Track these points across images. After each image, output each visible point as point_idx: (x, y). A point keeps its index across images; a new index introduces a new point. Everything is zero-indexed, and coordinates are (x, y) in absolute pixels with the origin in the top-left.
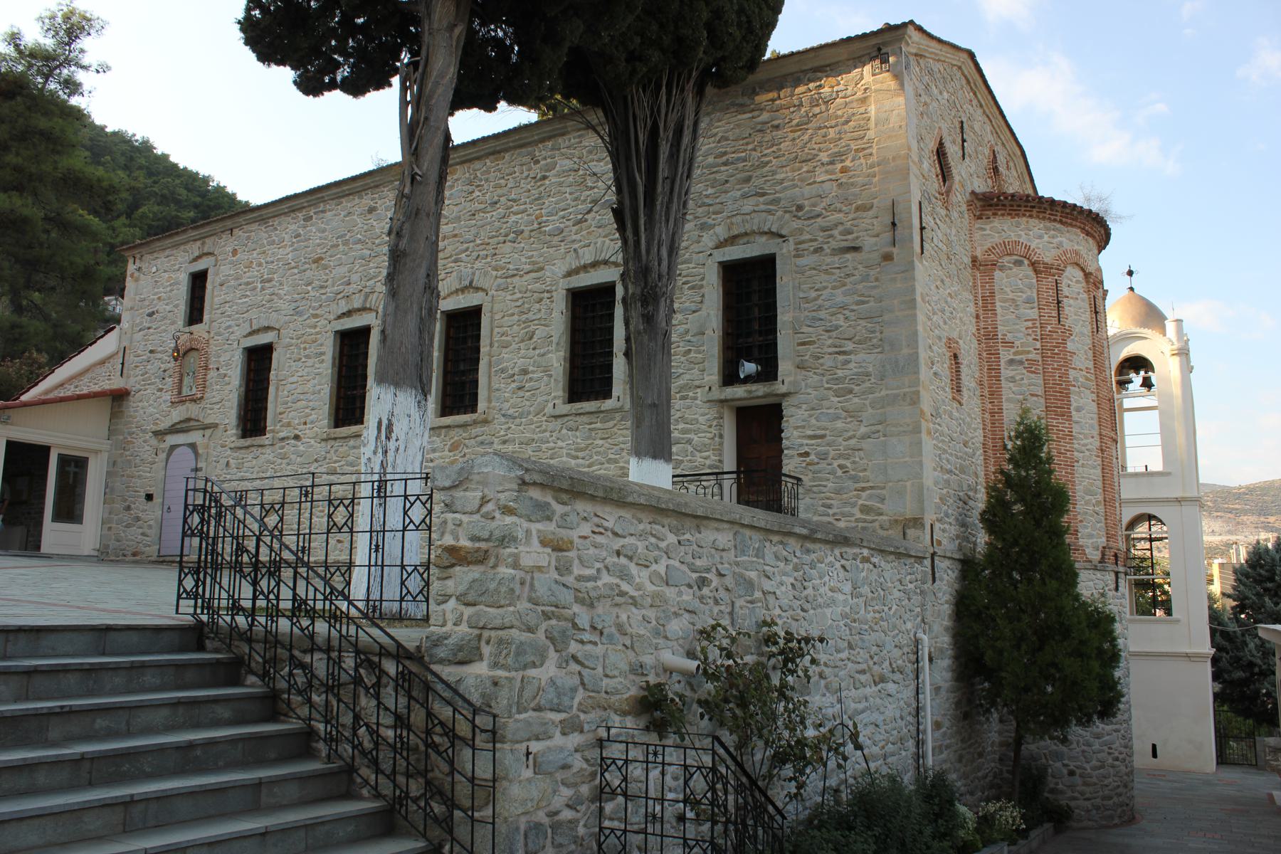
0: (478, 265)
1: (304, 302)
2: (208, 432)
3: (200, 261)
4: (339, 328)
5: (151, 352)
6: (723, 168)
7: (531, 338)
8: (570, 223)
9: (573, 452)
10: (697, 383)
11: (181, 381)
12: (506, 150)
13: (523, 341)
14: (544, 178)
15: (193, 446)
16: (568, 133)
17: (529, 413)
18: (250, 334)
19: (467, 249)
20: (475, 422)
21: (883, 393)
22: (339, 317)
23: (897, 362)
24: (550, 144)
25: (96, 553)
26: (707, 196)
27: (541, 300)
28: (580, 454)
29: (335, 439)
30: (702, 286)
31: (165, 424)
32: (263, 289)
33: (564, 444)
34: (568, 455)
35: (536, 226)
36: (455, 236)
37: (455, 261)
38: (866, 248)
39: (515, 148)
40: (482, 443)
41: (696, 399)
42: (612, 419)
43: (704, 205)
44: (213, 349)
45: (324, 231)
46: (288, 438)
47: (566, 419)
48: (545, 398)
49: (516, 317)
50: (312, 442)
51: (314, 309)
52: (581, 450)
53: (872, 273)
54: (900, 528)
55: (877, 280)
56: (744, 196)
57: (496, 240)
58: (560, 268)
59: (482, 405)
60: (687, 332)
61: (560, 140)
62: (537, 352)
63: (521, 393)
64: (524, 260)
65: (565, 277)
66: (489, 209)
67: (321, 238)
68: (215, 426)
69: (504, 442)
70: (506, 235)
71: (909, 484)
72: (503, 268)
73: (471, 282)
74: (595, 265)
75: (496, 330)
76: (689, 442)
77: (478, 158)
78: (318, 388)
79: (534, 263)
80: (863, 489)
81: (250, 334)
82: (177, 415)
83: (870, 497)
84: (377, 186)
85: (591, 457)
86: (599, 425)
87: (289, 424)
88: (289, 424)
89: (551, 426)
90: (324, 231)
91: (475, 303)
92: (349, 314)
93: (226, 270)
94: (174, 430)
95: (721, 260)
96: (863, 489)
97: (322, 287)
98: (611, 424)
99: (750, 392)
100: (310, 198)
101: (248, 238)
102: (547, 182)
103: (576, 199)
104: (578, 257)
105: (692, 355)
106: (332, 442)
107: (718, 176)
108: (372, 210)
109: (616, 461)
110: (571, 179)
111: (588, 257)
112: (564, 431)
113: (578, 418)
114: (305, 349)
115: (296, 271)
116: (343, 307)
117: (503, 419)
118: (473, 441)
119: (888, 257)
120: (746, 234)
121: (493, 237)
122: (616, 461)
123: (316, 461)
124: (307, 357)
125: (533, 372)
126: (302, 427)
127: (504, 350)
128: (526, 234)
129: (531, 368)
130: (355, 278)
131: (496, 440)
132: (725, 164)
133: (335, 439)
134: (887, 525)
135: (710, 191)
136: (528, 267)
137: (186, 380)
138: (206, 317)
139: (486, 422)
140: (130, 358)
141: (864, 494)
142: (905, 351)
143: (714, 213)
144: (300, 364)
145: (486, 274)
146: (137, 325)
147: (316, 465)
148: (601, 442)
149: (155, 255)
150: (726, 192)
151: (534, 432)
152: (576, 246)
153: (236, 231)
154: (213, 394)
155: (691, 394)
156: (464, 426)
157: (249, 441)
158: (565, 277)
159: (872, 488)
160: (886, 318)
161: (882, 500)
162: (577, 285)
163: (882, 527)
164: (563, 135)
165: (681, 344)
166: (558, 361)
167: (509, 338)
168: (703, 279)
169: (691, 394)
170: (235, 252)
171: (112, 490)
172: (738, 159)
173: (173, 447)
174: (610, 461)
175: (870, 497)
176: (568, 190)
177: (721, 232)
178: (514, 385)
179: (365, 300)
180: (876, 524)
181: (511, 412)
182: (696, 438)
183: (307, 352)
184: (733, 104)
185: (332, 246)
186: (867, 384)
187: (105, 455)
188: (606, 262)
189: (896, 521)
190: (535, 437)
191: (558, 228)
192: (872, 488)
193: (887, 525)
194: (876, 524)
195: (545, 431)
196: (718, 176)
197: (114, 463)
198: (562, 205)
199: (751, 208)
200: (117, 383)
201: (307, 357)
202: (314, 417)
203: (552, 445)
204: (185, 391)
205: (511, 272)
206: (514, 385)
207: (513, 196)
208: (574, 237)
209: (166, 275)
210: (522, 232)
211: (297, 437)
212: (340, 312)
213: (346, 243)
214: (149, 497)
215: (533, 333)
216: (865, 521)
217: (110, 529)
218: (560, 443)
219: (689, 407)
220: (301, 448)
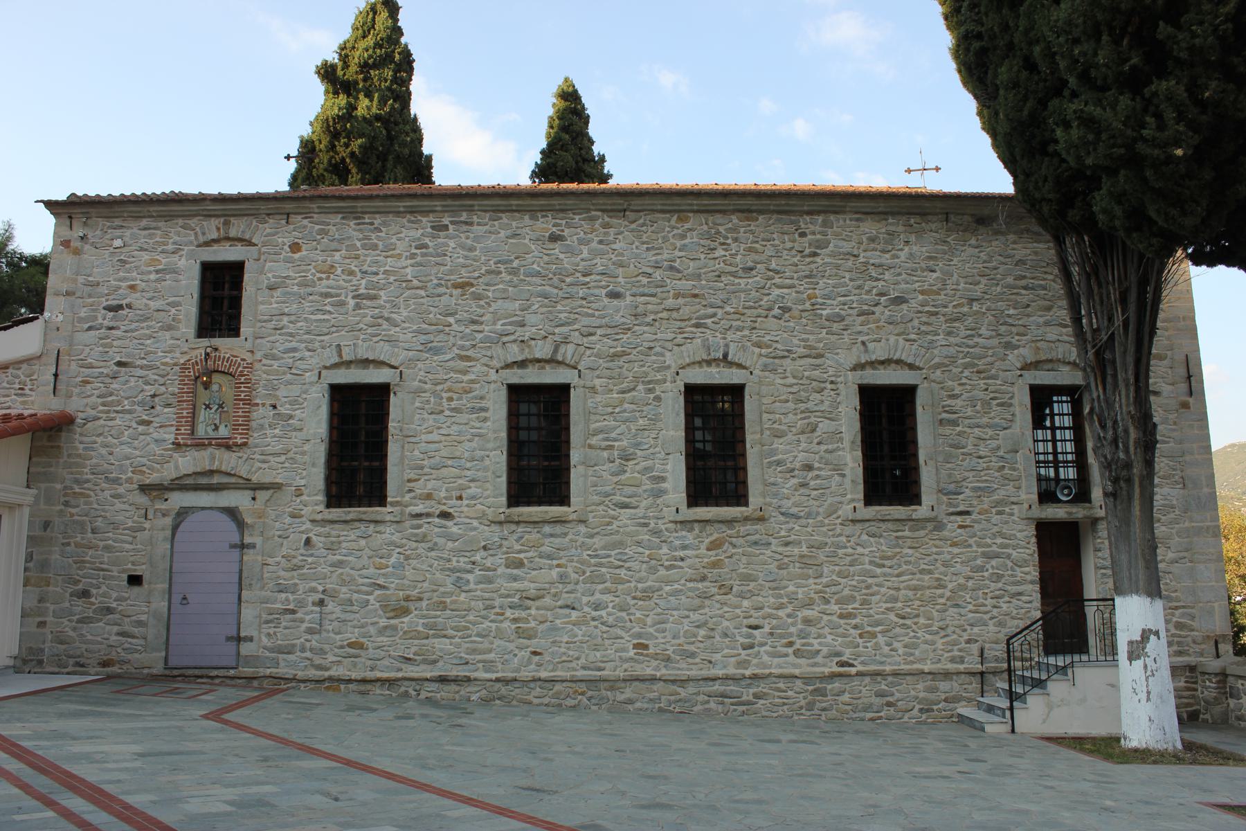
0: (730, 336)
1: (441, 337)
2: (262, 496)
3: (216, 247)
4: (515, 380)
5: (120, 364)
6: (1023, 292)
7: (813, 431)
8: (855, 312)
9: (877, 560)
10: (1013, 499)
11: (194, 415)
12: (760, 212)
13: (803, 433)
14: (815, 254)
15: (232, 513)
16: (844, 212)
17: (818, 513)
18: (335, 366)
19: (714, 315)
20: (746, 519)
21: (1187, 524)
22: (507, 366)
23: (1199, 498)
24: (820, 219)
25: (11, 662)
26: (1009, 316)
27: (822, 390)
28: (887, 563)
29: (518, 523)
30: (1011, 405)
31: (167, 473)
32: (358, 306)
33: (866, 551)
34: (871, 563)
35: (808, 306)
36: (695, 296)
37: (697, 326)
38: (1165, 394)
39: (779, 212)
40: (756, 543)
41: (1012, 514)
42: (923, 528)
43: (1005, 324)
44: (260, 375)
45: (471, 249)
46: (428, 515)
47: (867, 524)
48: (839, 499)
49: (791, 405)
50: (475, 523)
51: (462, 348)
52: (888, 558)
53: (1170, 416)
54: (1213, 643)
55: (1175, 423)
56: (1047, 324)
57: (755, 312)
58: (848, 358)
59: (755, 499)
60: (998, 448)
61: (832, 217)
62: (823, 447)
63: (802, 490)
64: (796, 341)
65: (854, 369)
66: (741, 273)
67: (466, 257)
68: (276, 487)
69: (787, 544)
70: (770, 309)
71: (1216, 605)
72: (768, 347)
73: (725, 356)
74: (885, 363)
75: (765, 416)
76: (1009, 556)
77: (723, 212)
78: (479, 453)
79: (811, 347)
80: (1176, 608)
81: (335, 366)
82: (186, 463)
83: (1183, 615)
84: (562, 211)
85: (900, 566)
86: (907, 533)
87: (429, 497)
88: (429, 497)
89: (848, 530)
90: (471, 249)
91: (736, 381)
92: (522, 364)
93: (275, 269)
94: (179, 485)
95: (1032, 382)
96: (1176, 608)
97: (474, 322)
98: (922, 533)
99: (1070, 513)
100: (449, 202)
101: (321, 232)
102: (818, 259)
103: (859, 287)
104: (866, 351)
105: (1006, 471)
106: (513, 527)
107: (1019, 298)
108: (554, 238)
109: (930, 572)
110: (850, 263)
111: (879, 352)
112: (865, 537)
113: (881, 524)
114: (450, 399)
115: (422, 293)
116: (515, 353)
117: (782, 518)
118: (741, 541)
119: (1185, 405)
120: (1051, 361)
121: (751, 308)
122: (930, 572)
123: (485, 548)
124: (456, 410)
125: (819, 469)
126: (454, 502)
127: (776, 440)
128: (796, 313)
129: (816, 465)
130: (531, 319)
131: (774, 541)
132: (1025, 288)
133: (518, 523)
134: (1199, 640)
135: (1012, 312)
136: (802, 351)
137: (203, 415)
138: (928, 478)
139: (762, 519)
140: (71, 368)
141: (1177, 612)
142: (1206, 490)
143: (1018, 334)
144: (441, 418)
145: (744, 348)
146: (81, 320)
147: (483, 553)
148: (910, 551)
149: (117, 222)
150: (1028, 316)
151: (825, 535)
152: (865, 338)
153: (293, 218)
154: (267, 437)
155: (1007, 510)
156: (730, 522)
157: (336, 513)
158: (854, 369)
159: (1184, 607)
160: (1188, 458)
161: (1193, 618)
162: (872, 382)
163: (1194, 642)
164: (836, 213)
165: (994, 459)
166: (854, 460)
167: (784, 427)
168: (1011, 398)
169: (1007, 510)
170: (295, 248)
171: (44, 565)
172: (1041, 286)
173: (183, 513)
174: (922, 572)
175: (1183, 615)
176: (847, 275)
177: (1027, 354)
178: (795, 481)
179: (556, 350)
180: (1189, 639)
181: (794, 510)
182: (1014, 554)
183: (454, 404)
184: (1028, 231)
185: (489, 272)
186: (1172, 515)
187: (27, 511)
188: (899, 362)
189: (1208, 637)
190: (828, 540)
191: (838, 315)
192: (1184, 607)
193: (1199, 640)
194: (1189, 639)
195: (840, 535)
196: (1019, 298)
197: (46, 525)
198: (842, 290)
199: (1055, 337)
200: (40, 403)
201: (456, 410)
202: (474, 490)
203: (850, 550)
204: (201, 431)
205: (781, 354)
206: (795, 481)
207: (773, 266)
208: (860, 328)
209: (146, 256)
210: (790, 310)
211: (445, 515)
212: (510, 360)
213: (514, 272)
214: (135, 580)
215: (817, 426)
216: (1180, 636)
217: (42, 624)
218: (860, 550)
219: (1006, 523)
220: (455, 529)
